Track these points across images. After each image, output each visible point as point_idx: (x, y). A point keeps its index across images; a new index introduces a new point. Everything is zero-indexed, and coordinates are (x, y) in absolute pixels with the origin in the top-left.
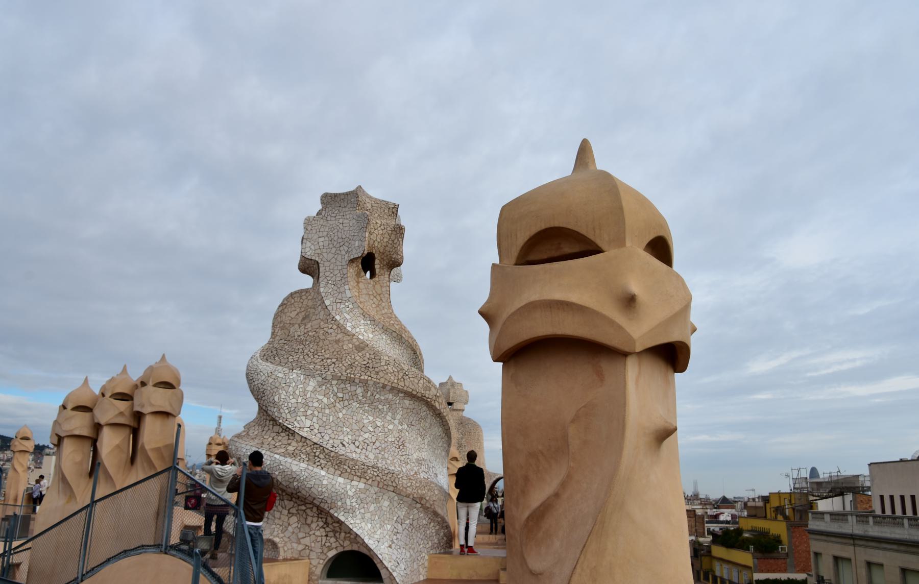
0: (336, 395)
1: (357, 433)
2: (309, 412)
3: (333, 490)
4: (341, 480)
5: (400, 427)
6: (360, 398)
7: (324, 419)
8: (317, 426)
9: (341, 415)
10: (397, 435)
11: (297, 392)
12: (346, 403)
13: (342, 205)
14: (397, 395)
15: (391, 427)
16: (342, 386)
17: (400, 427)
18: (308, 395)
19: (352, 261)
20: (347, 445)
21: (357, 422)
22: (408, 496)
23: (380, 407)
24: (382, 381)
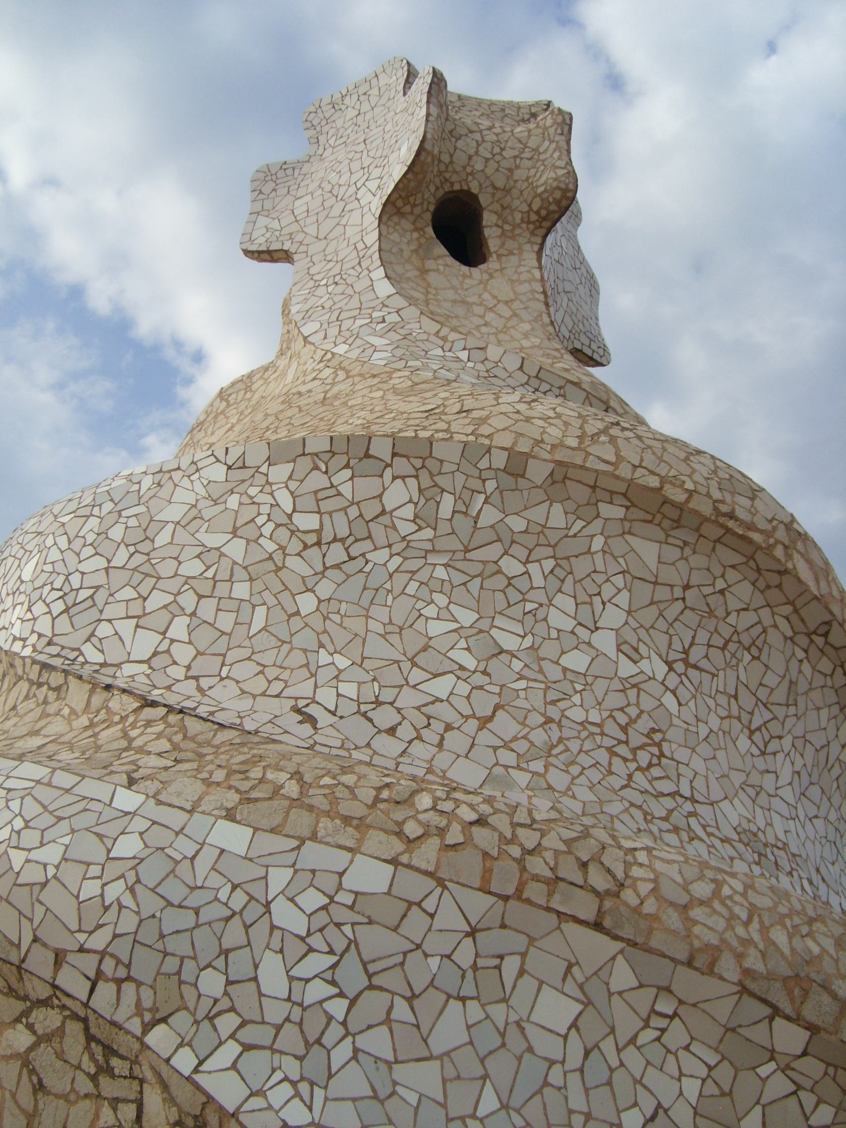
0: (287, 523)
1: (392, 676)
2: (157, 600)
3: (174, 891)
4: (233, 837)
5: (627, 669)
6: (405, 528)
7: (226, 622)
8: (184, 654)
9: (307, 603)
10: (615, 700)
11: (116, 533)
12: (337, 553)
13: (366, 107)
14: (586, 511)
15: (577, 661)
16: (318, 480)
17: (627, 669)
18: (163, 538)
19: (394, 207)
20: (324, 719)
21: (394, 630)
22: (700, 960)
23: (512, 567)
24: (506, 440)
